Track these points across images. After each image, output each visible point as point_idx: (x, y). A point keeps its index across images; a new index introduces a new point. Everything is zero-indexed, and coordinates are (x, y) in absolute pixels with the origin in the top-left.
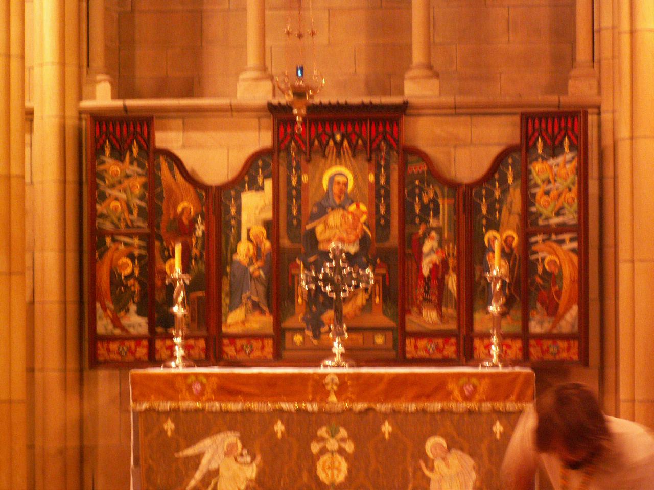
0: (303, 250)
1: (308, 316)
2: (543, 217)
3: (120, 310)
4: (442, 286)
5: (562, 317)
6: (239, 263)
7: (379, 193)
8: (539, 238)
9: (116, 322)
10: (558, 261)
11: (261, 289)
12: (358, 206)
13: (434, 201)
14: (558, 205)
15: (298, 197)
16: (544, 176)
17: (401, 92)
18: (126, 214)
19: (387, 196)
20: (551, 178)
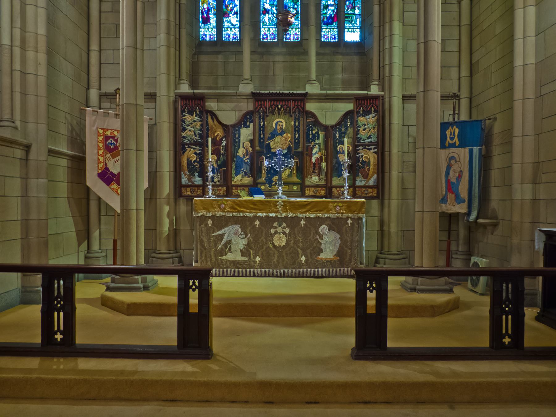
0: (265, 152)
1: (267, 178)
2: (362, 139)
3: (191, 175)
4: (320, 167)
5: (370, 179)
6: (238, 156)
7: (296, 129)
8: (361, 148)
9: (189, 180)
10: (368, 156)
11: (248, 167)
12: (287, 135)
13: (317, 133)
15: (263, 131)
16: (363, 123)
17: (305, 90)
18: (194, 137)
19: (299, 131)
20: (366, 123)
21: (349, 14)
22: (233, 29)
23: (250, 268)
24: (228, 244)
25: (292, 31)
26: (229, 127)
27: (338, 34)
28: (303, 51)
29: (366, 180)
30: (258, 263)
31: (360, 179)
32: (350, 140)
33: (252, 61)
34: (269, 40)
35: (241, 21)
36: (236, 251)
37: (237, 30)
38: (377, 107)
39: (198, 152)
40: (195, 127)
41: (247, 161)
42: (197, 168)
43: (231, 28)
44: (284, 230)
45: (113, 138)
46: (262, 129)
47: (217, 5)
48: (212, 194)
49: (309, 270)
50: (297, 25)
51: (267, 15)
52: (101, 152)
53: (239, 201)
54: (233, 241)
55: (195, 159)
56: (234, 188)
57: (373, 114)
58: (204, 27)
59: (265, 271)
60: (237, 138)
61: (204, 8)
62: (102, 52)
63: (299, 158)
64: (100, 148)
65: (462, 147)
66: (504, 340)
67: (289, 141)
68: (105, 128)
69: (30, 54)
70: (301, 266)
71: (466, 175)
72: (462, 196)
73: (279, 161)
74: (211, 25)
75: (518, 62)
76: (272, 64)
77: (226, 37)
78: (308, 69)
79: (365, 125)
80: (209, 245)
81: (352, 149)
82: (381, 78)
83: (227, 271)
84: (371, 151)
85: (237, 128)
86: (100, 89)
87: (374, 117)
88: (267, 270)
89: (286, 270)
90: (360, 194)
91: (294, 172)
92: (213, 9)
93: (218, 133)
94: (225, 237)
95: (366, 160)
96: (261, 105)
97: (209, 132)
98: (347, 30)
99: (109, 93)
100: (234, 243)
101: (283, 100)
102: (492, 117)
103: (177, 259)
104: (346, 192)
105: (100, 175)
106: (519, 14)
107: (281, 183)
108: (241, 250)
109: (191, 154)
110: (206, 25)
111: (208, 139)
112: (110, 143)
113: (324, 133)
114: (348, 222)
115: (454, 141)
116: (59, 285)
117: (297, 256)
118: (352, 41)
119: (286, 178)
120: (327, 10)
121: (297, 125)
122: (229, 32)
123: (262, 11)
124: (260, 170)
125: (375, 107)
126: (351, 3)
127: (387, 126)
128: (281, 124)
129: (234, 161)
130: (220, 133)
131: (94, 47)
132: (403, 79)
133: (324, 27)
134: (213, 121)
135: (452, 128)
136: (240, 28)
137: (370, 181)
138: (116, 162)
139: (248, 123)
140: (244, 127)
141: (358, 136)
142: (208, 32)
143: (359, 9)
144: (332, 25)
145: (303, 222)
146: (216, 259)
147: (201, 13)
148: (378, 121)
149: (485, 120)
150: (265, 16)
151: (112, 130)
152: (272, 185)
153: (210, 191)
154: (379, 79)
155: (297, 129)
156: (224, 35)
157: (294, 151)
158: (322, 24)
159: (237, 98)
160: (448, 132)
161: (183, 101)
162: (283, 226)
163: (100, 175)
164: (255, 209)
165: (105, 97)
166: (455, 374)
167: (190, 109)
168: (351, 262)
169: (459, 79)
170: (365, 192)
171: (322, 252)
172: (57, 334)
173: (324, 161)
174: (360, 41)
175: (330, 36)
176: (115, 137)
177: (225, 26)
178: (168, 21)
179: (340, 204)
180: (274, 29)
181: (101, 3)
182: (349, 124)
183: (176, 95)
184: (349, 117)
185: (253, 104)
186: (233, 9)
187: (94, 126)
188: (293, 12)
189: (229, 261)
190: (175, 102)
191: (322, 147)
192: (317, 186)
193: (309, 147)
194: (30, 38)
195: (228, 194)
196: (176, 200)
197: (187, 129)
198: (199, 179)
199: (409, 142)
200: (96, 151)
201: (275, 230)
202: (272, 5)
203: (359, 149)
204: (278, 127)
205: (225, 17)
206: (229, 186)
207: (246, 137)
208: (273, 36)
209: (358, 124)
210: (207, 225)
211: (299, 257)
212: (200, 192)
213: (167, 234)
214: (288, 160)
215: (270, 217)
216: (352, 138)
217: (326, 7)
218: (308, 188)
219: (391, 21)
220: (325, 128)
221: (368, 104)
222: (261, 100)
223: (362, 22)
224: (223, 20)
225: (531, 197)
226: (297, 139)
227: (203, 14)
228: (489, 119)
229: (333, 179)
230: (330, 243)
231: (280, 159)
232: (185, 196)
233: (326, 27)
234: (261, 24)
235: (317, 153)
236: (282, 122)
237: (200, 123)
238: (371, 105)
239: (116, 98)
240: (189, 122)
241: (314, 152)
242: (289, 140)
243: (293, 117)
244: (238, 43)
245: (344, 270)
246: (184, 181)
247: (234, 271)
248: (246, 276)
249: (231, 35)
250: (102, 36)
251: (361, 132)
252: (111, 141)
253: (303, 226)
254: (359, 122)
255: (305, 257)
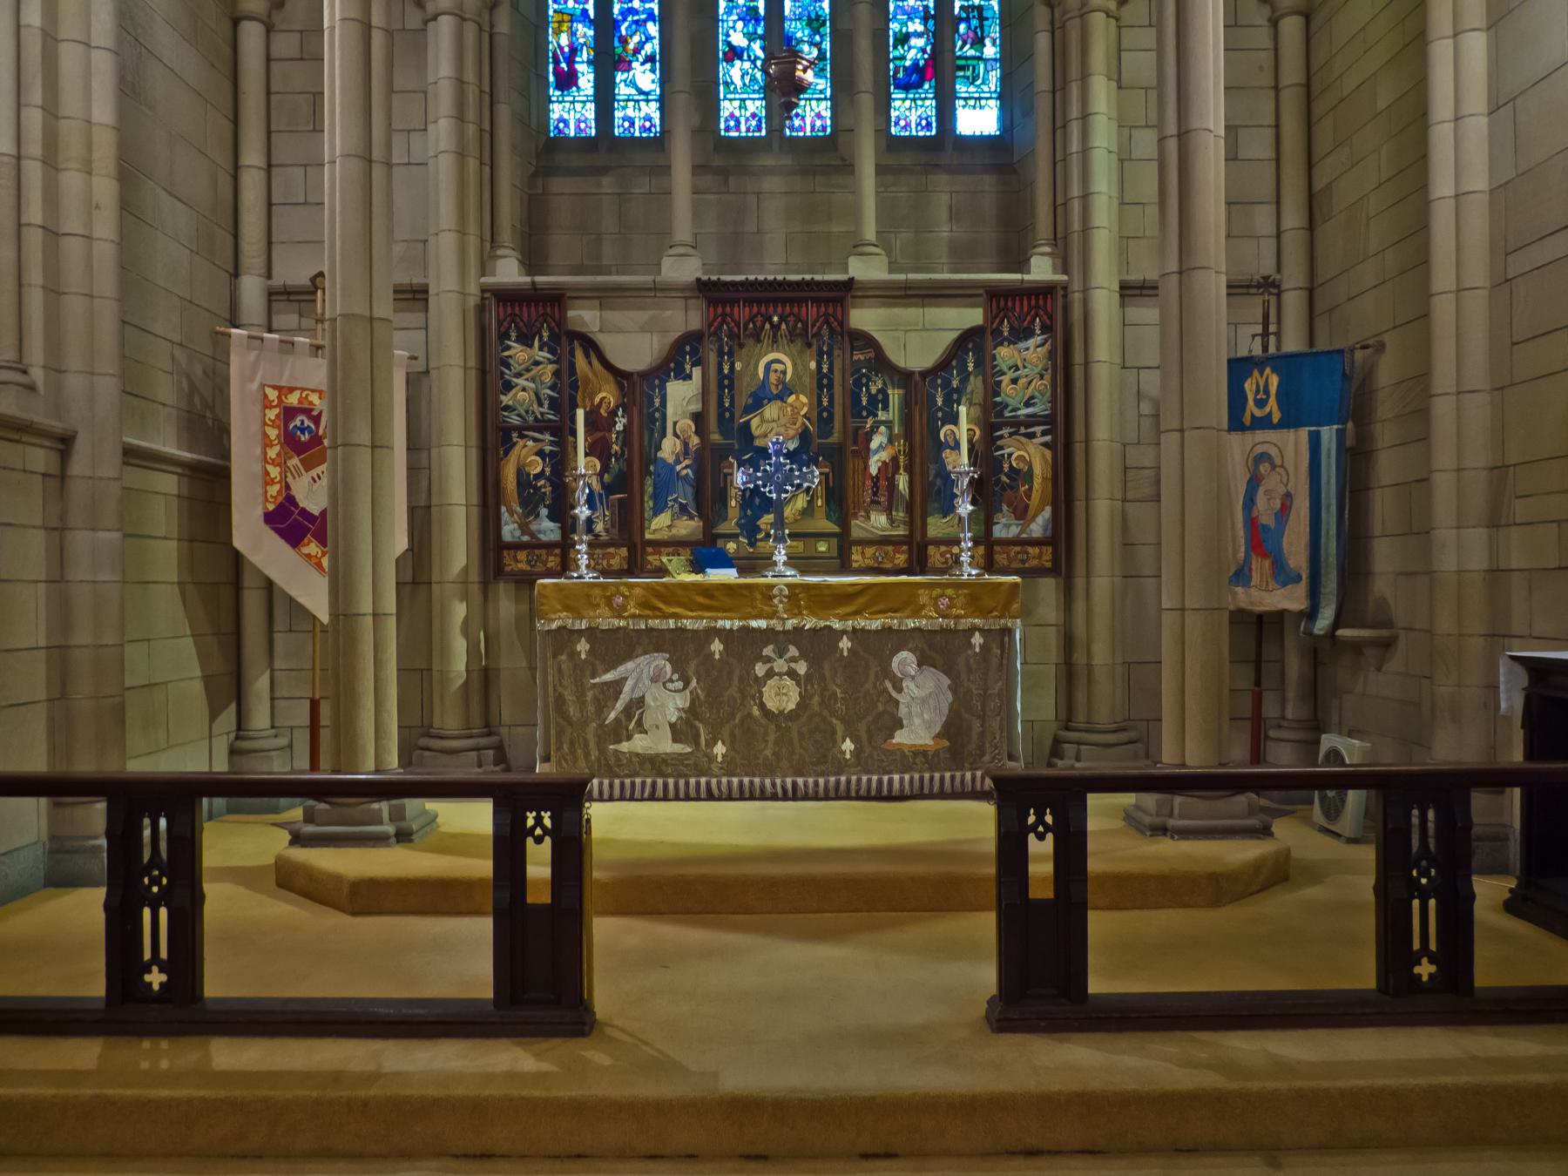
0: (736, 447)
1: (743, 521)
2: (1010, 408)
4: (892, 486)
5: (1033, 519)
6: (663, 460)
7: (823, 382)
8: (1005, 431)
9: (524, 528)
11: (689, 490)
12: (798, 398)
13: (883, 391)
14: (1029, 393)
15: (731, 387)
16: (1010, 362)
18: (535, 406)
19: (830, 386)
21: (967, 58)
22: (643, 104)
23: (698, 776)
24: (634, 709)
25: (808, 108)
26: (635, 376)
27: (938, 115)
28: (838, 162)
29: (1021, 522)
30: (720, 759)
31: (1004, 520)
32: (976, 411)
33: (696, 191)
34: (744, 134)
35: (663, 82)
36: (657, 727)
37: (654, 105)
38: (1051, 317)
39: (548, 448)
40: (538, 379)
41: (687, 474)
42: (545, 493)
43: (638, 101)
44: (793, 665)
45: (307, 412)
46: (726, 382)
47: (596, 37)
48: (588, 567)
49: (864, 778)
50: (821, 92)
51: (737, 63)
52: (272, 453)
53: (665, 585)
54: (649, 700)
55: (539, 469)
56: (650, 550)
57: (1039, 338)
58: (560, 99)
59: (741, 784)
60: (657, 410)
61: (561, 48)
62: (275, 171)
63: (832, 463)
64: (271, 441)
65: (1288, 427)
66: (1417, 970)
67: (804, 416)
68: (283, 384)
69: (72, 180)
70: (840, 767)
71: (1302, 505)
72: (1292, 563)
73: (776, 471)
74: (581, 93)
75: (1443, 186)
76: (752, 199)
77: (623, 126)
78: (855, 214)
79: (1017, 369)
80: (581, 712)
81: (981, 436)
82: (1059, 236)
83: (633, 784)
84: (1035, 441)
85: (657, 382)
86: (269, 276)
87: (1042, 345)
88: (746, 780)
89: (800, 781)
90: (1005, 562)
91: (820, 503)
92: (585, 48)
93: (604, 394)
94: (627, 688)
95: (1022, 465)
96: (545, 315)
97: (577, 392)
98: (962, 102)
99: (294, 286)
100: (652, 704)
101: (784, 301)
102: (1370, 342)
103: (491, 752)
104: (965, 558)
105: (269, 518)
106: (1441, 52)
107: (783, 533)
108: (672, 726)
109: (527, 456)
110: (566, 93)
111: (575, 414)
112: (299, 428)
113: (901, 391)
114: (973, 641)
115: (1268, 409)
116: (155, 831)
117: (832, 739)
118: (978, 133)
119: (796, 520)
120: (906, 48)
121: (825, 370)
122: (630, 112)
123: (724, 53)
124: (722, 497)
125: (1045, 317)
126: (973, 28)
127: (1078, 372)
128: (779, 367)
129: (650, 474)
130: (607, 395)
131: (252, 156)
132: (1121, 237)
133: (897, 95)
134: (590, 363)
135: (1261, 374)
136: (663, 102)
137: (1033, 526)
138: (315, 481)
139: (688, 367)
140: (677, 378)
141: (998, 399)
142: (572, 112)
143: (994, 44)
144: (920, 91)
145: (845, 644)
146: (602, 751)
147: (551, 60)
148: (1051, 355)
149: (1352, 351)
150: (733, 66)
151: (303, 390)
152: (757, 540)
153: (584, 560)
154: (1055, 239)
155: (825, 381)
156: (616, 121)
157: (819, 444)
158: (892, 87)
159: (655, 296)
160: (1249, 386)
161: (505, 307)
162: (789, 655)
163: (269, 518)
164: (709, 608)
165: (285, 297)
166: (1281, 1067)
167: (525, 330)
168: (982, 755)
169: (1278, 236)
170: (1020, 556)
171: (902, 727)
172: (150, 972)
173: (902, 471)
174: (998, 133)
175: (913, 118)
176: (312, 410)
177: (619, 94)
178: (460, 82)
179: (949, 592)
180: (758, 103)
181: (272, 34)
182: (971, 367)
183: (483, 291)
184: (970, 346)
185: (699, 313)
186: (642, 48)
187: (252, 379)
188: (810, 53)
189: (638, 755)
190: (481, 309)
191: (896, 431)
192: (884, 541)
193: (860, 432)
194: (71, 134)
195: (633, 567)
196: (485, 584)
197: (517, 385)
198: (547, 525)
199: (1140, 416)
200: (258, 451)
201: (768, 665)
202: (751, 37)
203: (1001, 437)
204: (773, 378)
205: (618, 71)
206: (635, 545)
207: (682, 405)
208: (754, 123)
209: (996, 366)
210: (574, 654)
211: (835, 742)
212: (553, 562)
213: (460, 681)
214: (800, 470)
215: (754, 630)
216: (980, 404)
217: (904, 39)
218: (859, 548)
219: (1085, 77)
220: (905, 378)
221: (1025, 309)
222: (724, 302)
223: (1003, 79)
224: (615, 78)
225: (1485, 566)
226: (825, 409)
227: (556, 62)
228: (1364, 347)
229: (930, 520)
230: (924, 701)
231: (779, 466)
232: (512, 573)
233: (903, 96)
234: (721, 88)
235: (884, 449)
236: (784, 364)
237: (551, 367)
238: (1033, 312)
239: (314, 301)
240: (520, 365)
241: (874, 445)
242: (803, 413)
243: (815, 347)
244: (658, 144)
245: (963, 777)
246: (509, 531)
247: (654, 784)
248: (688, 798)
249: (637, 121)
250: (273, 128)
251: (1007, 388)
252: (302, 422)
253: (845, 654)
254: (1000, 361)
255: (852, 741)
